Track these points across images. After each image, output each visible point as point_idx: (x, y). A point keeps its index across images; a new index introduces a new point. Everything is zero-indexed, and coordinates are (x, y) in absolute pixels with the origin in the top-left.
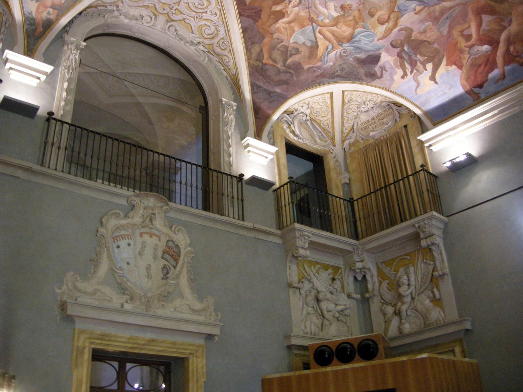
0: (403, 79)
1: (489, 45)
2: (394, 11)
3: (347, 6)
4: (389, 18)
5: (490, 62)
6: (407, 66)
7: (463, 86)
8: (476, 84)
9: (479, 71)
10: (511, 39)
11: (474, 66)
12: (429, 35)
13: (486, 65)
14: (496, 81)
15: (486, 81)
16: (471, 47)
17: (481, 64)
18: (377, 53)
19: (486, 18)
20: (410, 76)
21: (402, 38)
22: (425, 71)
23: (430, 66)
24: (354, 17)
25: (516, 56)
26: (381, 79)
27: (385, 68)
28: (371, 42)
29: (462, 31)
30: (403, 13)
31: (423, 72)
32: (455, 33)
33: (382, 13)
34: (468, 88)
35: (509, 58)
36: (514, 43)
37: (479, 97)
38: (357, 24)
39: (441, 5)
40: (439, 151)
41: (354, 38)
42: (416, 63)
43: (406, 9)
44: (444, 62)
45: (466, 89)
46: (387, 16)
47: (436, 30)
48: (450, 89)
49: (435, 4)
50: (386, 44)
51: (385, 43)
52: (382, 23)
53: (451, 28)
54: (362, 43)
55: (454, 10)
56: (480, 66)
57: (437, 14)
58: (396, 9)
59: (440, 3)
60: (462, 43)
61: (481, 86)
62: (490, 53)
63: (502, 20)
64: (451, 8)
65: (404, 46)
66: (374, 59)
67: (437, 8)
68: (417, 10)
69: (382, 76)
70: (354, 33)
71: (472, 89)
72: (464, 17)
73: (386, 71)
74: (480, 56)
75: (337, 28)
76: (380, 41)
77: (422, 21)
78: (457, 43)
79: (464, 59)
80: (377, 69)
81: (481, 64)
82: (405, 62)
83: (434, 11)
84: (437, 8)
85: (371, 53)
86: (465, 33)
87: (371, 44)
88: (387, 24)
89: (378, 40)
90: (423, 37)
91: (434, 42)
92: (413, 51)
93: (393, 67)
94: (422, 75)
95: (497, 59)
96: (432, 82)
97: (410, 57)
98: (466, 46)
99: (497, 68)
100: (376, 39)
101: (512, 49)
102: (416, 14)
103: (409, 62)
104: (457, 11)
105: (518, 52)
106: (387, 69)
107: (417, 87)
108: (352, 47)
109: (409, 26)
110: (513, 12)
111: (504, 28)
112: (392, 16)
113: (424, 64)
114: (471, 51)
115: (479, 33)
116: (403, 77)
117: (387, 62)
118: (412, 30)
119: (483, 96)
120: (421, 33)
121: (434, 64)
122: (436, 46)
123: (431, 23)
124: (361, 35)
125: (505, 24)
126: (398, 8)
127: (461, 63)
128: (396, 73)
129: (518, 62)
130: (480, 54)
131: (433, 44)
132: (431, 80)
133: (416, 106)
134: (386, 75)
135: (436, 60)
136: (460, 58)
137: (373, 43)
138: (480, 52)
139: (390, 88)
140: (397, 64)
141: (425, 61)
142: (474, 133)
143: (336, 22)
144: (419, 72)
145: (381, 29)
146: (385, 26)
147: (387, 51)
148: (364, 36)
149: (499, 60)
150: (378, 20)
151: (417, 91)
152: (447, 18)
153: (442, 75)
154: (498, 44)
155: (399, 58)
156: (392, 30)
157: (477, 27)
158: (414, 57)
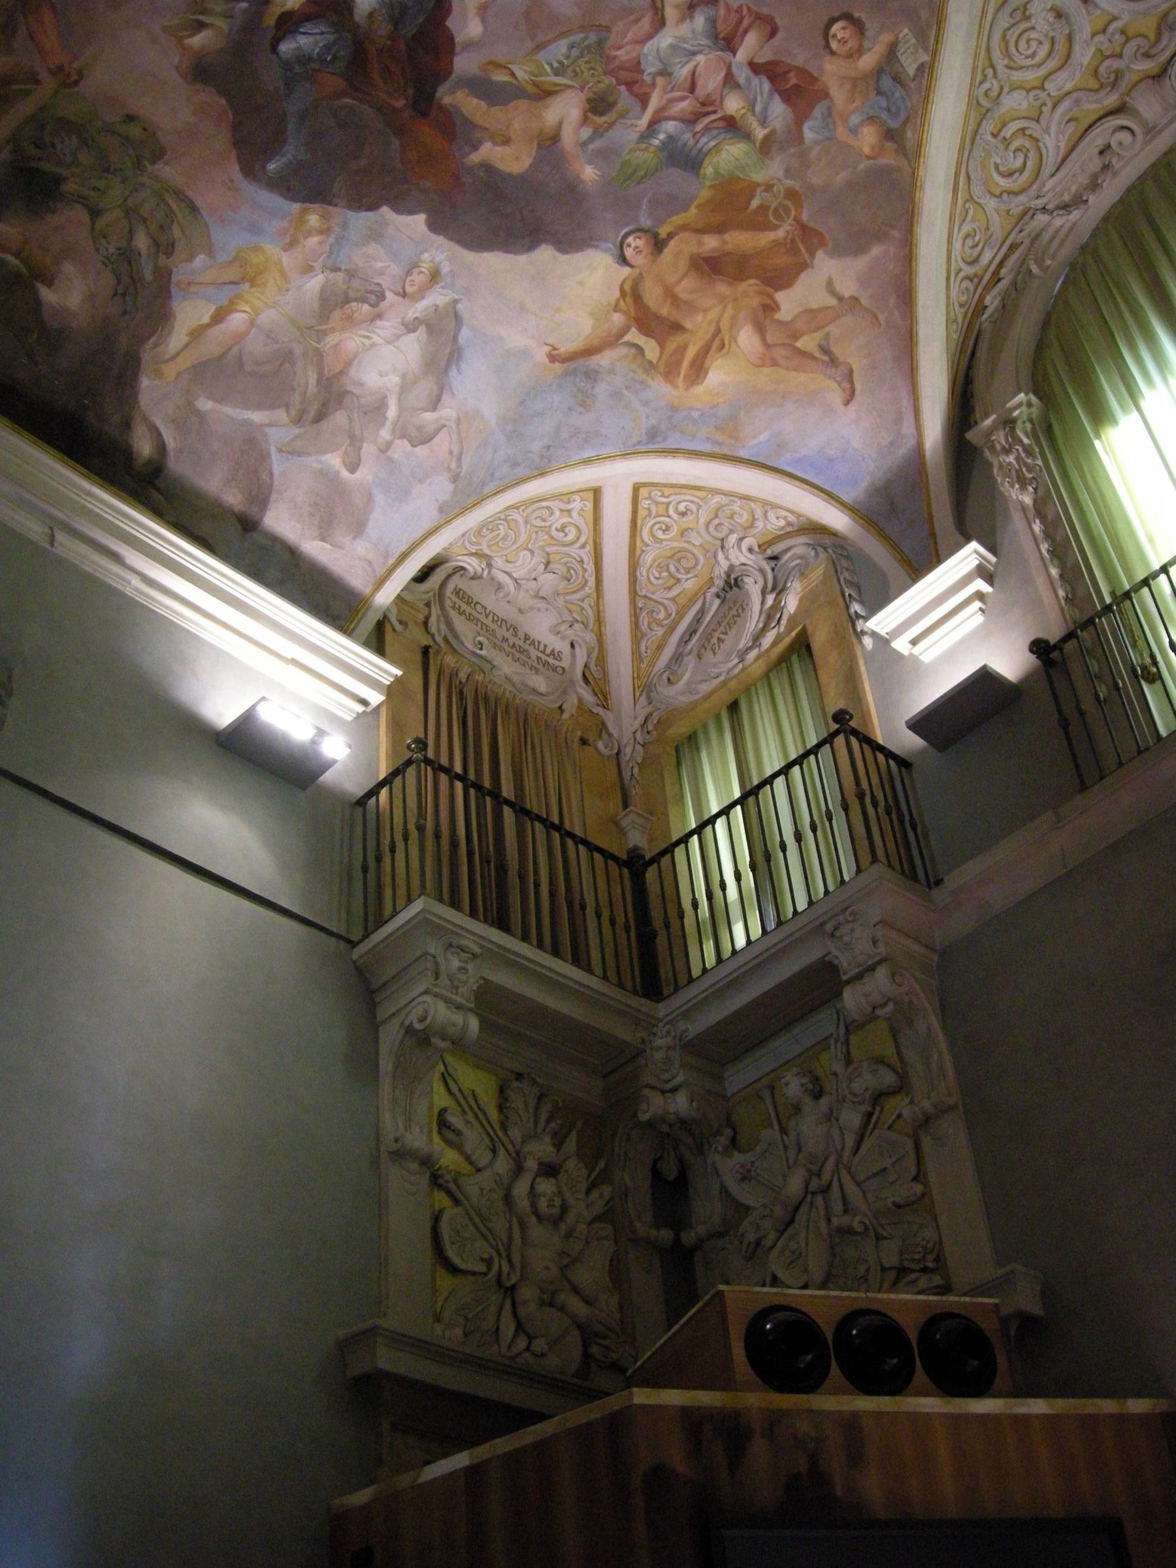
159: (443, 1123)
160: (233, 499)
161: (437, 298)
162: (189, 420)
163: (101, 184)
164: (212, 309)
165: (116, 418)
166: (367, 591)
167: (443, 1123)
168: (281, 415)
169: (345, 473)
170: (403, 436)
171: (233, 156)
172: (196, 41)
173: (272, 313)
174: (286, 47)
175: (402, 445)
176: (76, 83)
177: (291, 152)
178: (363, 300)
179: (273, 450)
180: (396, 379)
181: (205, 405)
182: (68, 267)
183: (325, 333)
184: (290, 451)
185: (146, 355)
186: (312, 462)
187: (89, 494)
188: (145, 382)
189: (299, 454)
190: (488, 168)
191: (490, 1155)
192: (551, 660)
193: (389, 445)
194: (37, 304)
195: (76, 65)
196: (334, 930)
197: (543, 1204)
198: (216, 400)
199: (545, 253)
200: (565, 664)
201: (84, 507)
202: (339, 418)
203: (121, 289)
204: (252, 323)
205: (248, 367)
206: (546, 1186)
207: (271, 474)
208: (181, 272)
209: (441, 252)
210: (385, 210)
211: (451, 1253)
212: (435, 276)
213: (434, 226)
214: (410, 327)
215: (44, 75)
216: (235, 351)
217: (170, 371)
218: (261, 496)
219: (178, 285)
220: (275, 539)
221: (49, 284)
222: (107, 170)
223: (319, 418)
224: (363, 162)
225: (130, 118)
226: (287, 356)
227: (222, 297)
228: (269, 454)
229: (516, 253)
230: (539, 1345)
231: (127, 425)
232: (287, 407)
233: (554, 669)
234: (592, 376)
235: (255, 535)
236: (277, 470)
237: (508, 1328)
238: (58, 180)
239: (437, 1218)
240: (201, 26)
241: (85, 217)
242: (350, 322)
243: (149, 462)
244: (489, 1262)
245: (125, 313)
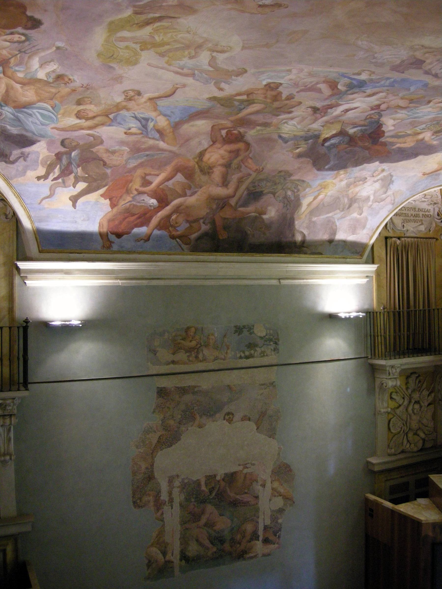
0: (38, 180)
1: (158, 201)
2: (107, 116)
3: (66, 79)
4: (94, 117)
5: (144, 217)
6: (57, 172)
7: (101, 225)
8: (115, 230)
9: (127, 220)
10: (182, 207)
11: (128, 212)
12: (114, 158)
13: (139, 218)
14: (138, 239)
15: (128, 233)
16: (140, 193)
17: (133, 215)
18: (35, 138)
19: (179, 177)
20: (49, 182)
21: (81, 143)
22: (72, 187)
23: (82, 186)
24: (59, 92)
25: (172, 226)
26: (9, 165)
27: (27, 157)
28: (42, 124)
29: (146, 175)
30: (113, 124)
31: (70, 186)
32: (140, 172)
33: (91, 109)
34: (105, 230)
35: (165, 224)
36: (180, 213)
37: (110, 247)
38: (52, 99)
39: (157, 142)
40: (34, 288)
41: (28, 108)
42: (71, 173)
43: (122, 123)
44: (102, 191)
45: (101, 230)
46: (95, 115)
47: (125, 159)
48: (84, 220)
49: (153, 139)
50: (58, 137)
51: (58, 136)
52: (78, 116)
53: (141, 165)
54: (30, 119)
55: (162, 153)
56: (133, 215)
57: (143, 147)
58: (111, 116)
59: (157, 140)
60: (136, 185)
61: (119, 235)
62: (152, 208)
63: (190, 188)
64: (162, 150)
65: (74, 150)
66: (25, 141)
67: (151, 142)
68: (130, 131)
69: (13, 162)
70: (35, 104)
71: (107, 233)
72: (161, 165)
73: (25, 160)
74: (141, 206)
75: (22, 87)
76: (56, 132)
77: (122, 143)
78: (131, 181)
79: (124, 200)
80: (16, 153)
81: (136, 214)
82: (58, 166)
83: (144, 143)
84: (151, 142)
85: (29, 135)
86: (148, 178)
87: (41, 127)
88: (84, 121)
89: (52, 128)
90: (105, 156)
91: (111, 167)
92: (78, 161)
93: (38, 162)
94: (64, 189)
95: (154, 218)
96: (71, 203)
97: (70, 164)
98: (136, 190)
99: (147, 226)
100: (53, 125)
101: (174, 217)
102: (126, 133)
103: (63, 168)
104: (163, 156)
105: (176, 223)
106: (28, 159)
107: (47, 197)
108: (13, 115)
109: (104, 137)
110: (204, 187)
111: (185, 195)
112: (99, 119)
113: (77, 180)
114: (137, 197)
115: (160, 185)
116: (39, 178)
117: (38, 153)
118: (102, 142)
119: (115, 247)
120: (107, 151)
121: (88, 186)
122: (109, 171)
123: (128, 150)
124: (40, 111)
125: (188, 192)
126: (115, 118)
127: (118, 202)
128: (35, 170)
129: (170, 232)
130: (143, 204)
131: (107, 168)
132: (70, 199)
133: (30, 217)
134: (21, 164)
135: (95, 184)
136: (121, 197)
137: (44, 127)
138: (145, 203)
139: (12, 179)
140: (46, 162)
141: (82, 177)
142: (86, 287)
143: (32, 81)
144: (64, 184)
145: (73, 121)
146: (78, 121)
147: (51, 143)
148: (42, 115)
149: (155, 221)
150: (79, 112)
151: (44, 201)
152: (147, 155)
153: (87, 202)
154: (167, 205)
155: (55, 157)
156: (83, 129)
157: (163, 180)
158: (73, 167)
159: (391, 398)
160: (326, 237)
161: (385, 174)
162: (311, 225)
163: (275, 187)
164: (313, 197)
165: (290, 235)
166: (368, 241)
167: (391, 398)
168: (338, 211)
169: (358, 216)
170: (376, 202)
171: (314, 168)
172: (298, 151)
173: (332, 192)
174: (326, 144)
175: (375, 205)
176: (262, 171)
177: (332, 163)
178: (360, 181)
179: (336, 220)
180: (372, 192)
181: (314, 219)
182: (269, 208)
183: (349, 190)
184: (342, 218)
185: (296, 216)
186: (348, 218)
187: (287, 266)
188: (296, 222)
189: (344, 218)
190: (399, 148)
191: (403, 400)
192: (427, 213)
193: (371, 205)
194: (263, 219)
195: (261, 168)
196: (363, 356)
197: (415, 411)
198: (316, 217)
199: (420, 157)
200: (431, 213)
201: (286, 270)
202: (355, 205)
203: (285, 205)
204: (326, 196)
205: (326, 205)
206: (417, 406)
207: (336, 226)
208: (302, 194)
209: (385, 166)
210: (365, 165)
211: (391, 429)
212: (383, 170)
213: (381, 162)
214: (375, 182)
215: (251, 172)
216: (322, 203)
217: (303, 216)
218: (334, 233)
219: (302, 196)
220: (339, 241)
221: (265, 214)
222: (276, 184)
223: (350, 206)
224: (356, 158)
225: (280, 172)
226: (338, 198)
227: (316, 193)
228: (335, 222)
229: (411, 159)
230: (413, 445)
231: (293, 235)
232: (339, 209)
233: (428, 216)
234: (439, 174)
235: (333, 243)
236: (338, 224)
237: (405, 441)
238: (262, 192)
239: (389, 421)
240: (298, 148)
241: (272, 196)
242: (357, 186)
243: (301, 241)
244: (401, 428)
245: (288, 209)
